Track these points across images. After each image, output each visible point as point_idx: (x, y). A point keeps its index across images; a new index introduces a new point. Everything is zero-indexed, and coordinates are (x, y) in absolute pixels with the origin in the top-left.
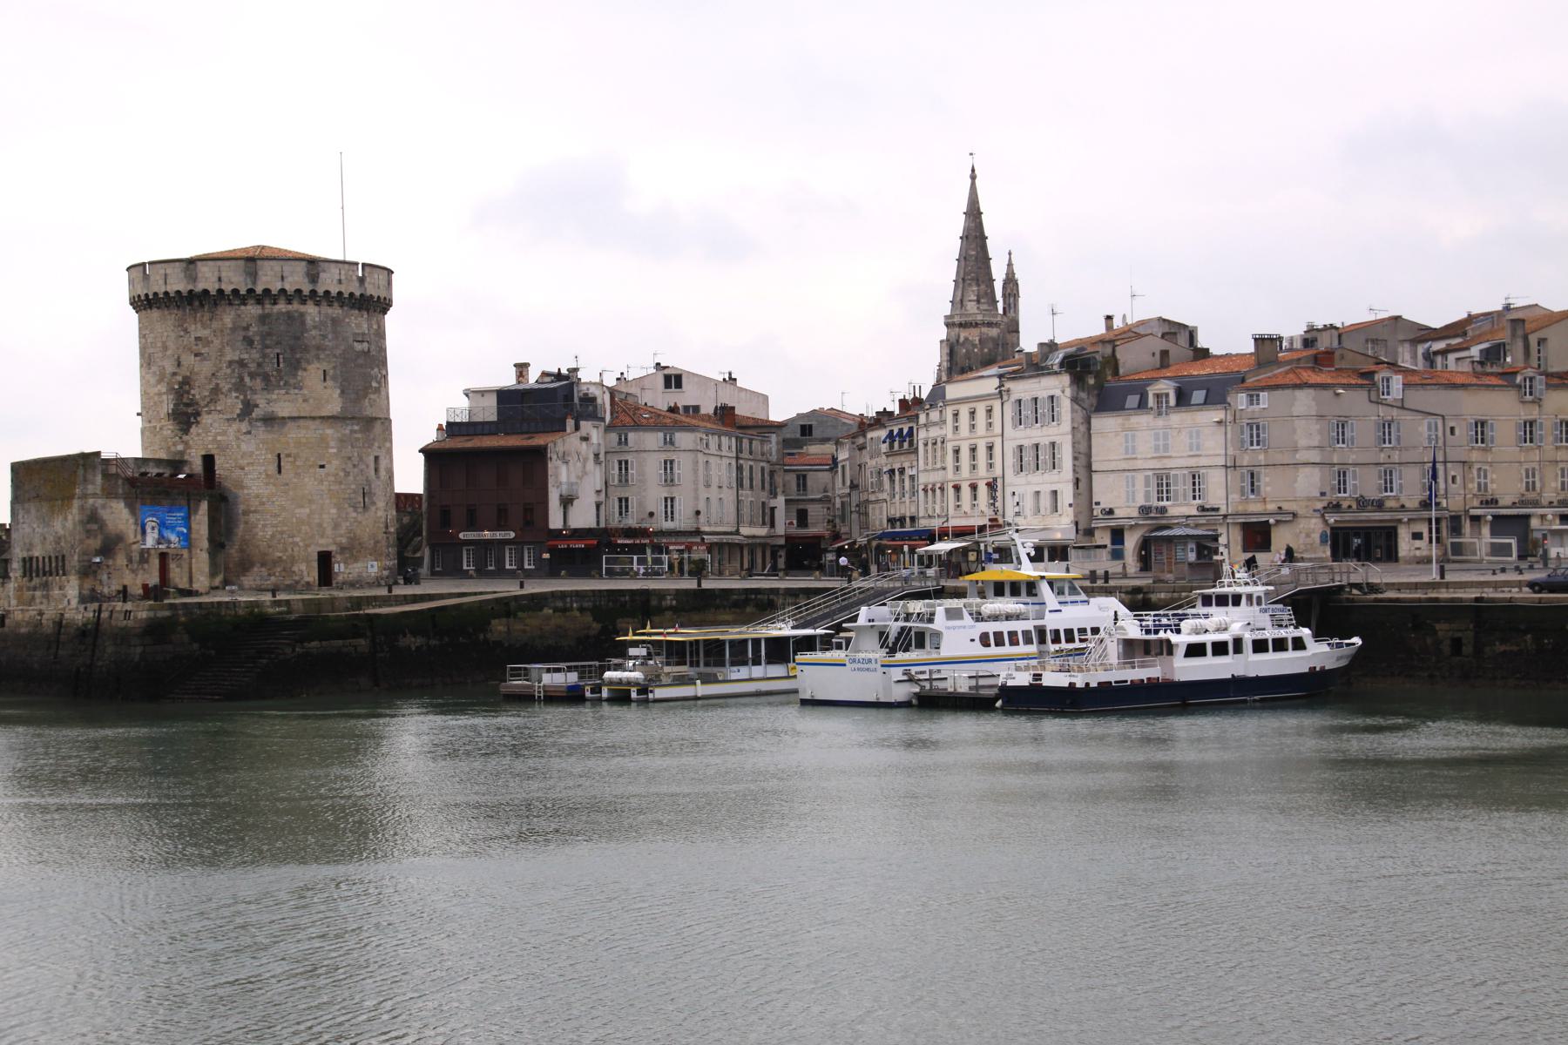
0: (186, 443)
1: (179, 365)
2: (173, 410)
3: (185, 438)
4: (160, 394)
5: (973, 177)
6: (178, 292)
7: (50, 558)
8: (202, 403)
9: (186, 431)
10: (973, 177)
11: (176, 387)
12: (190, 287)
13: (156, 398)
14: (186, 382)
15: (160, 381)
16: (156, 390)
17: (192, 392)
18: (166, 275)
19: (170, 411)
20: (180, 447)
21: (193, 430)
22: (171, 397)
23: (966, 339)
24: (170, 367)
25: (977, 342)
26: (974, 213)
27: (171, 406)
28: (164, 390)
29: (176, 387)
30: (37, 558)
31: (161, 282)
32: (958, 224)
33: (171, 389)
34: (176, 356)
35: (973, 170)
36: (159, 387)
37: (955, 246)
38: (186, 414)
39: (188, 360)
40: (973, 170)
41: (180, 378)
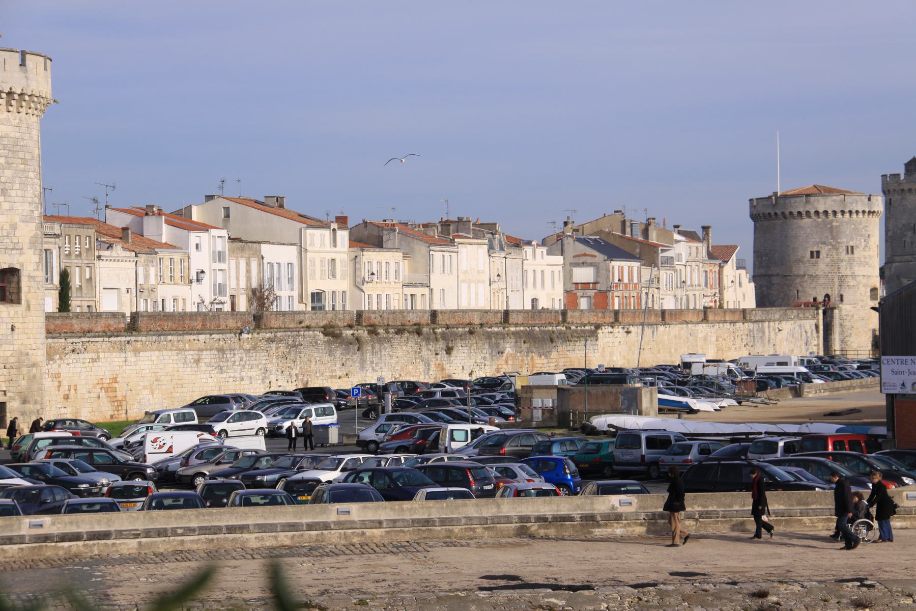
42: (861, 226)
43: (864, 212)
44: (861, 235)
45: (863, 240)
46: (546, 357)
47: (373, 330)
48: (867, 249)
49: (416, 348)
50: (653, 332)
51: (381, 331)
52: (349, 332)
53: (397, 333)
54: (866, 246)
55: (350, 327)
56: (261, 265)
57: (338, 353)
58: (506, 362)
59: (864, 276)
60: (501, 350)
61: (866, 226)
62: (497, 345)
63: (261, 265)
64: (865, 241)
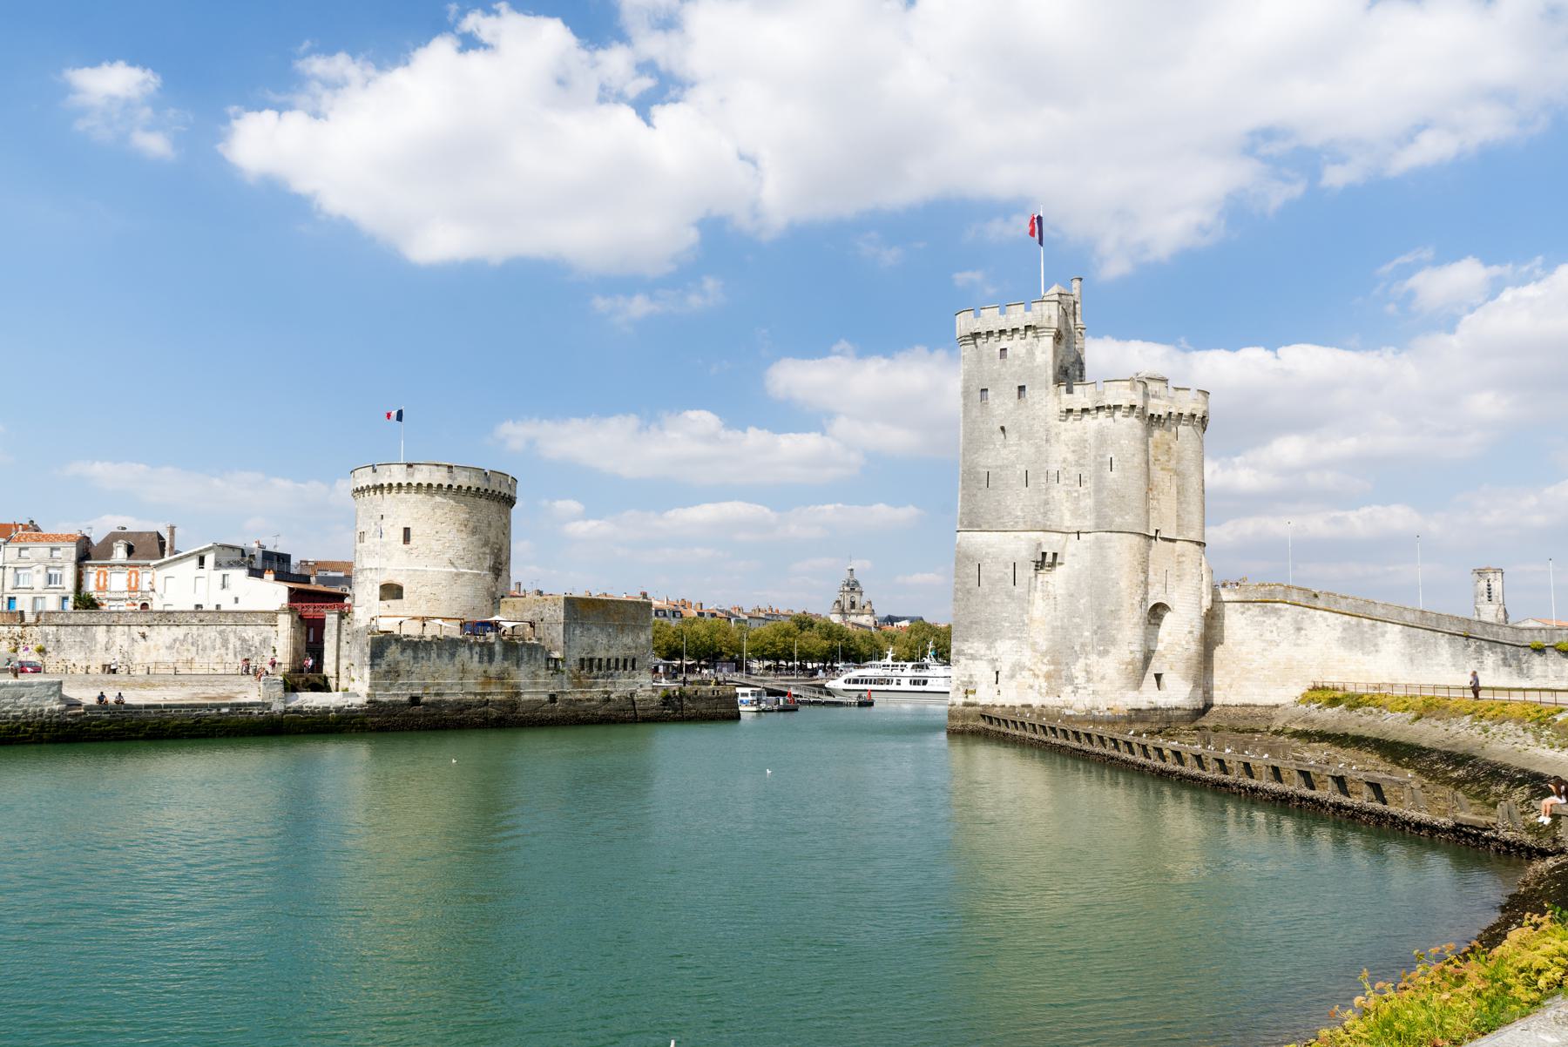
1: (497, 538)
4: (484, 553)
7: (617, 660)
13: (481, 555)
14: (500, 550)
15: (486, 544)
16: (481, 550)
20: (494, 589)
22: (492, 557)
27: (492, 563)
28: (488, 551)
30: (600, 660)
31: (498, 485)
33: (492, 553)
36: (484, 549)
38: (498, 568)
41: (498, 547)
44: (371, 517)
45: (373, 524)
64: (376, 524)
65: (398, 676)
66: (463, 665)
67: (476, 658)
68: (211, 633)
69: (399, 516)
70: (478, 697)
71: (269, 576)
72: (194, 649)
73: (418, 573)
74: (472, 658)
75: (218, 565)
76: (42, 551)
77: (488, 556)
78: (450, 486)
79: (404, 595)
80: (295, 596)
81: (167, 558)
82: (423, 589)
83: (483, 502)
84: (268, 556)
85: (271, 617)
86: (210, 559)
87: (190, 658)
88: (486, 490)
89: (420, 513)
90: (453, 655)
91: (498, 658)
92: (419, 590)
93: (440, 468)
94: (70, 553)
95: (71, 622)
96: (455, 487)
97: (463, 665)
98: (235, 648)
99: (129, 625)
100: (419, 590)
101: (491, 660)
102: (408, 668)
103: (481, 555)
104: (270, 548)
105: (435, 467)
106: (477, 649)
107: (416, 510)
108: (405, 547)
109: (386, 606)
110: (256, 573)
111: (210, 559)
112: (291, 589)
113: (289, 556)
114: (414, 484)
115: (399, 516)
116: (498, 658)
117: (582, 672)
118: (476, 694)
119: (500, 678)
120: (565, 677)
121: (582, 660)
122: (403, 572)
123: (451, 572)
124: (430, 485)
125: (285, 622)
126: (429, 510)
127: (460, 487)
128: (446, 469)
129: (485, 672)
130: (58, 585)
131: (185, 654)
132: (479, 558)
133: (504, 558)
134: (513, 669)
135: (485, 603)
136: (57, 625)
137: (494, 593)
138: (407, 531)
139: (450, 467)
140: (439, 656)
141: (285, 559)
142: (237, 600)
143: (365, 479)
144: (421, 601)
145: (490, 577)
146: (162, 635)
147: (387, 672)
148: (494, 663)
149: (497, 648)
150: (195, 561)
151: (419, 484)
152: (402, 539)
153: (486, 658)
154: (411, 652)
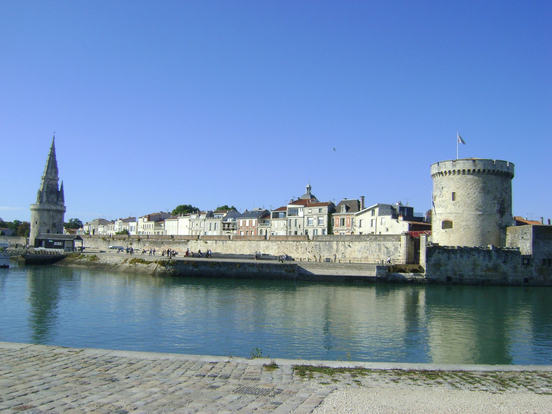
0: (502, 221)
1: (502, 195)
2: (499, 209)
3: (502, 219)
4: (494, 203)
5: (54, 138)
6: (505, 172)
8: (506, 208)
9: (502, 217)
10: (54, 138)
11: (501, 202)
12: (508, 171)
13: (492, 205)
14: (503, 201)
15: (495, 198)
16: (492, 202)
17: (505, 204)
18: (502, 165)
19: (498, 210)
20: (500, 222)
21: (504, 217)
22: (499, 205)
23: (52, 184)
24: (498, 195)
25: (55, 185)
26: (53, 149)
27: (499, 208)
28: (496, 202)
29: (501, 202)
32: (49, 152)
34: (501, 192)
35: (54, 137)
36: (494, 201)
37: (47, 158)
39: (504, 194)
40: (54, 137)
41: (502, 199)
42: (438, 182)
43: (450, 172)
45: (439, 191)
46: (159, 248)
47: (113, 239)
48: (441, 196)
49: (123, 243)
50: (223, 243)
51: (115, 239)
52: (107, 239)
53: (119, 239)
54: (440, 195)
55: (108, 238)
56: (129, 227)
57: (105, 243)
58: (146, 248)
59: (438, 214)
60: (145, 245)
61: (441, 182)
62: (144, 243)
63: (129, 227)
64: (440, 191)
65: (440, 266)
66: (474, 261)
67: (481, 258)
68: (374, 245)
69: (450, 187)
70: (483, 278)
71: (401, 218)
72: (368, 252)
73: (459, 215)
74: (479, 257)
75: (380, 214)
76: (316, 210)
77: (496, 205)
78: (474, 170)
79: (453, 226)
80: (411, 227)
81: (361, 211)
82: (462, 223)
83: (493, 177)
84: (402, 209)
85: (397, 238)
86: (377, 210)
87: (367, 256)
88: (494, 171)
89: (460, 185)
90: (468, 257)
91: (494, 258)
92: (460, 223)
93: (469, 161)
94: (325, 209)
95: (324, 240)
96: (477, 170)
97: (474, 261)
98: (384, 252)
99: (281, 241)
100: (460, 223)
101: (490, 257)
102: (445, 263)
103: (492, 205)
104: (404, 205)
105: (467, 161)
106: (482, 253)
107: (458, 183)
108: (453, 202)
109: (445, 231)
110: (395, 216)
111: (377, 210)
112: (410, 224)
113: (413, 208)
114: (456, 170)
115: (450, 187)
116: (494, 258)
117: (544, 267)
118: (482, 276)
119: (495, 268)
120: (534, 268)
121: (544, 260)
122: (452, 215)
123: (476, 214)
124: (464, 171)
125: (403, 239)
126: (464, 183)
127: (479, 170)
128: (472, 161)
129: (487, 265)
130: (322, 225)
131: (365, 254)
132: (491, 206)
133: (506, 205)
134: (501, 264)
135: (495, 229)
136: (320, 241)
137: (500, 224)
138: (453, 193)
139: (474, 161)
140: (461, 256)
141: (410, 210)
142: (387, 230)
143: (434, 170)
144: (461, 229)
145: (498, 216)
146: (357, 246)
147: (434, 264)
148: (491, 260)
149: (493, 253)
150: (370, 212)
151: (459, 171)
152: (452, 198)
153: (487, 258)
154: (447, 254)
